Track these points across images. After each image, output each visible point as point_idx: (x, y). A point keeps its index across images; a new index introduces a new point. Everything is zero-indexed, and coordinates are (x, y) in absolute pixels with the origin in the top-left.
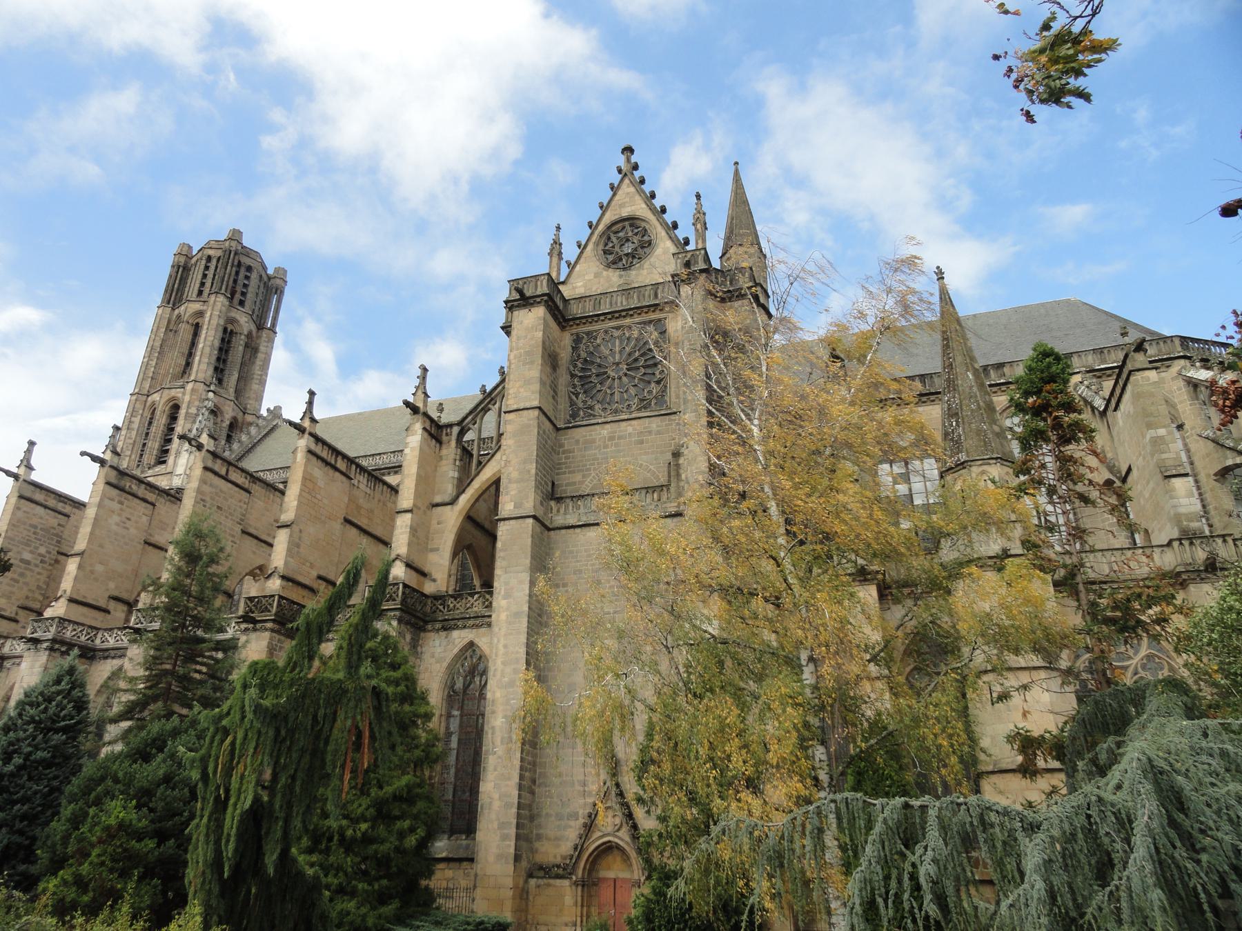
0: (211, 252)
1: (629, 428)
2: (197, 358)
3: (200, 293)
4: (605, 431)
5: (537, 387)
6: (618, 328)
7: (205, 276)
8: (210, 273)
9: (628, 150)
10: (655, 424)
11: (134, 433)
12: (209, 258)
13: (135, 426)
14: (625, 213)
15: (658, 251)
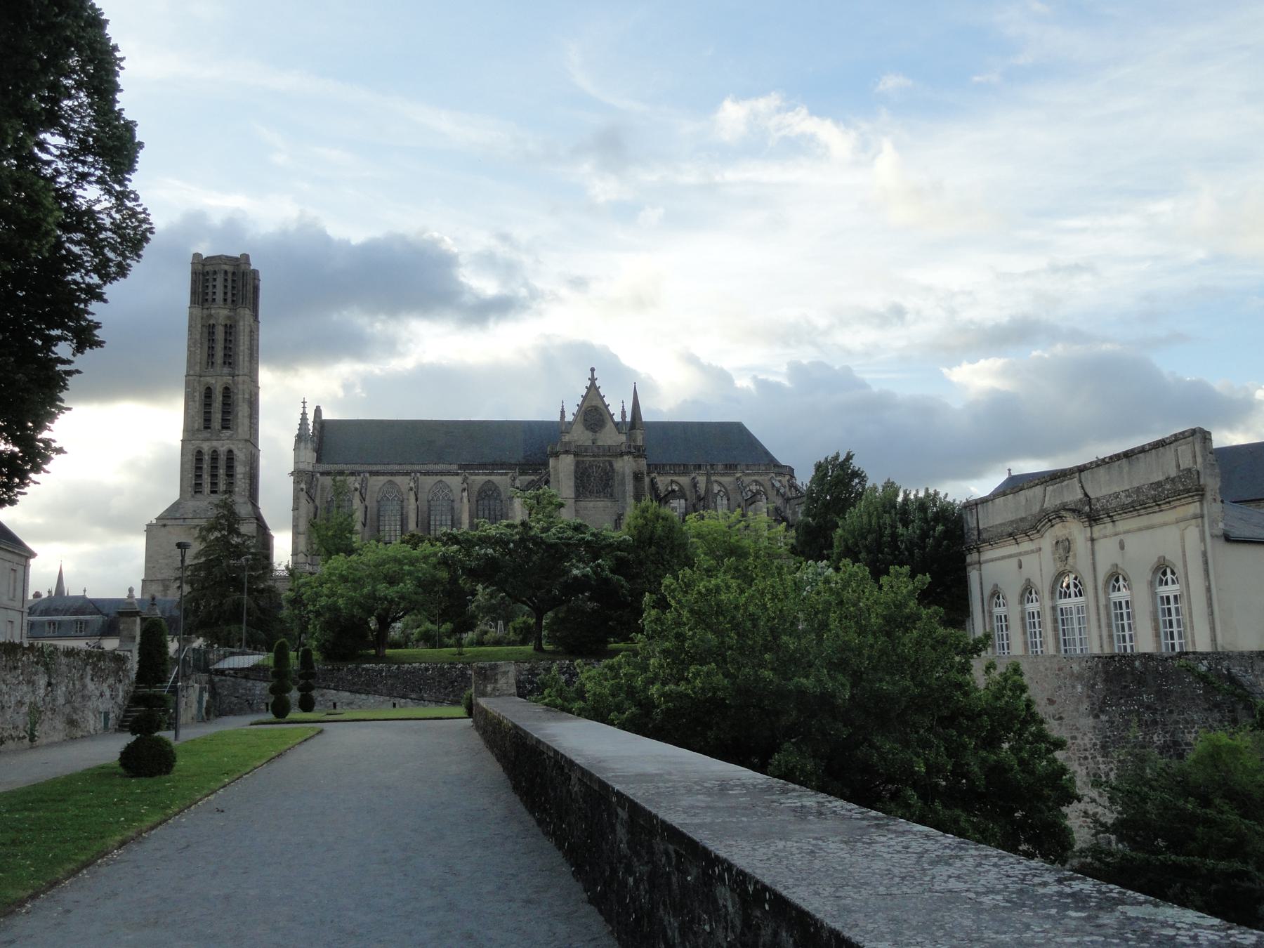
0: (226, 267)
1: (600, 504)
2: (241, 357)
3: (225, 300)
4: (591, 504)
5: (573, 489)
6: (594, 461)
7: (226, 287)
8: (229, 284)
9: (593, 370)
10: (609, 504)
11: (197, 404)
12: (226, 272)
13: (197, 398)
14: (594, 403)
15: (608, 426)
